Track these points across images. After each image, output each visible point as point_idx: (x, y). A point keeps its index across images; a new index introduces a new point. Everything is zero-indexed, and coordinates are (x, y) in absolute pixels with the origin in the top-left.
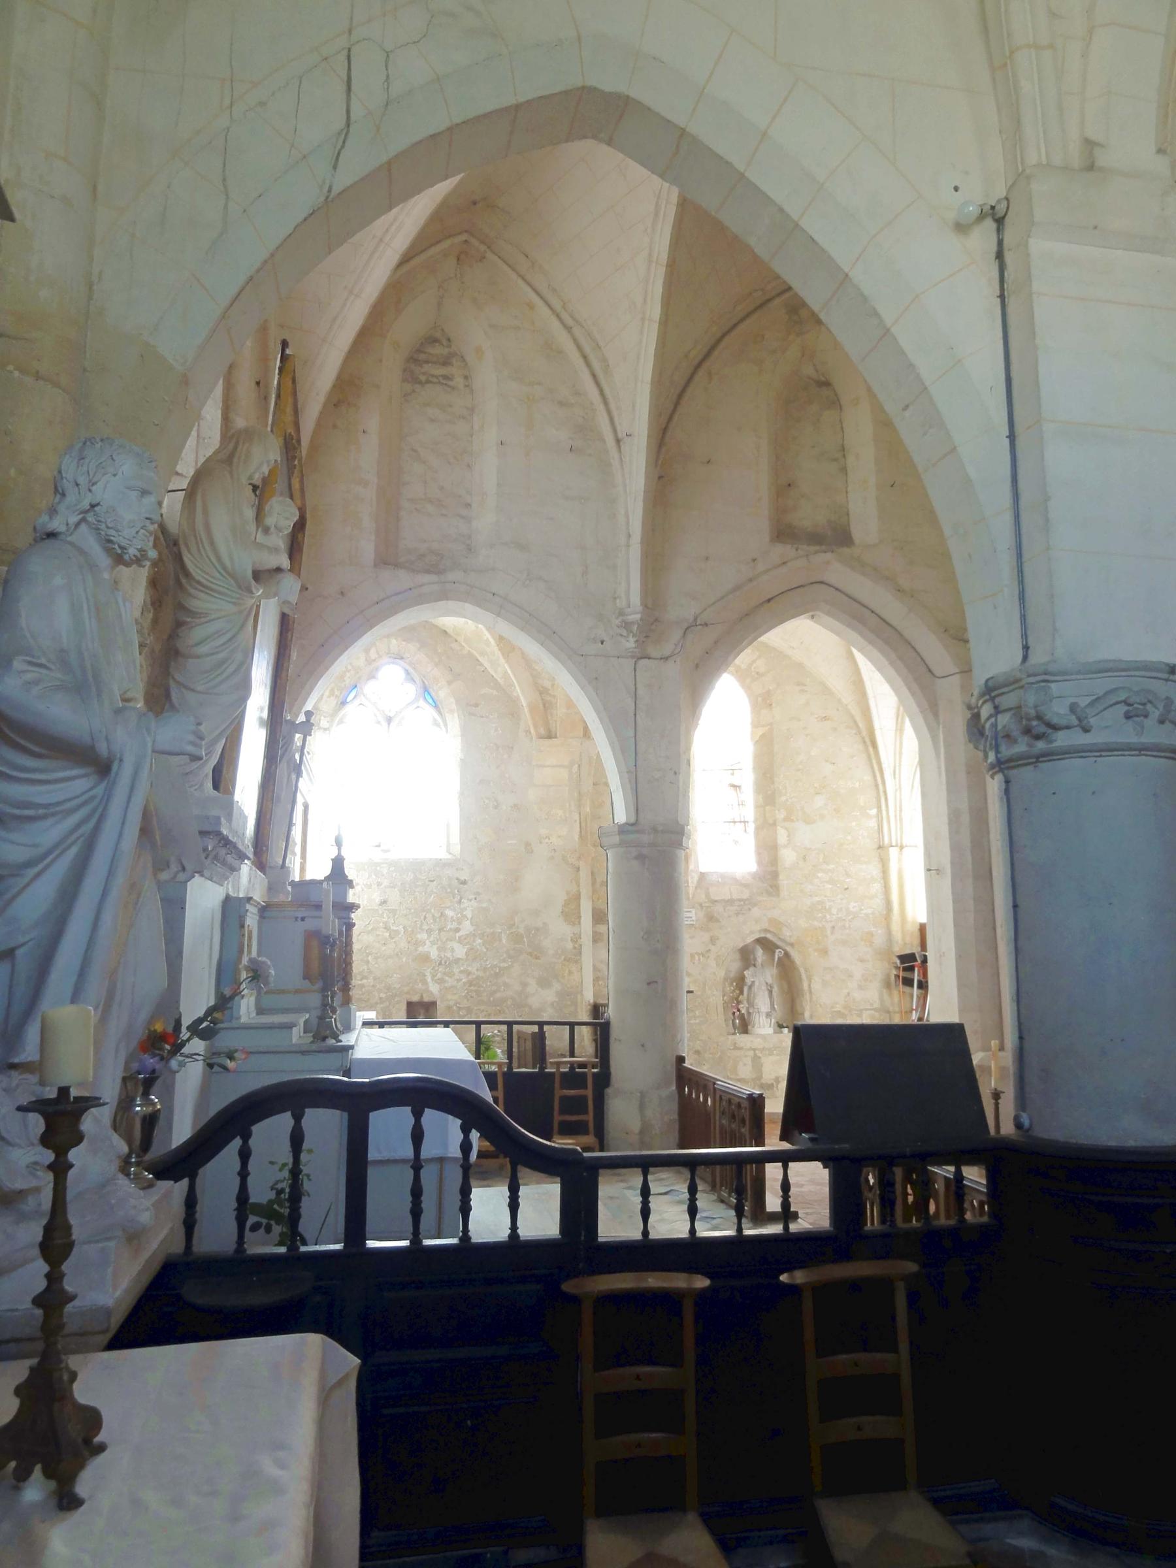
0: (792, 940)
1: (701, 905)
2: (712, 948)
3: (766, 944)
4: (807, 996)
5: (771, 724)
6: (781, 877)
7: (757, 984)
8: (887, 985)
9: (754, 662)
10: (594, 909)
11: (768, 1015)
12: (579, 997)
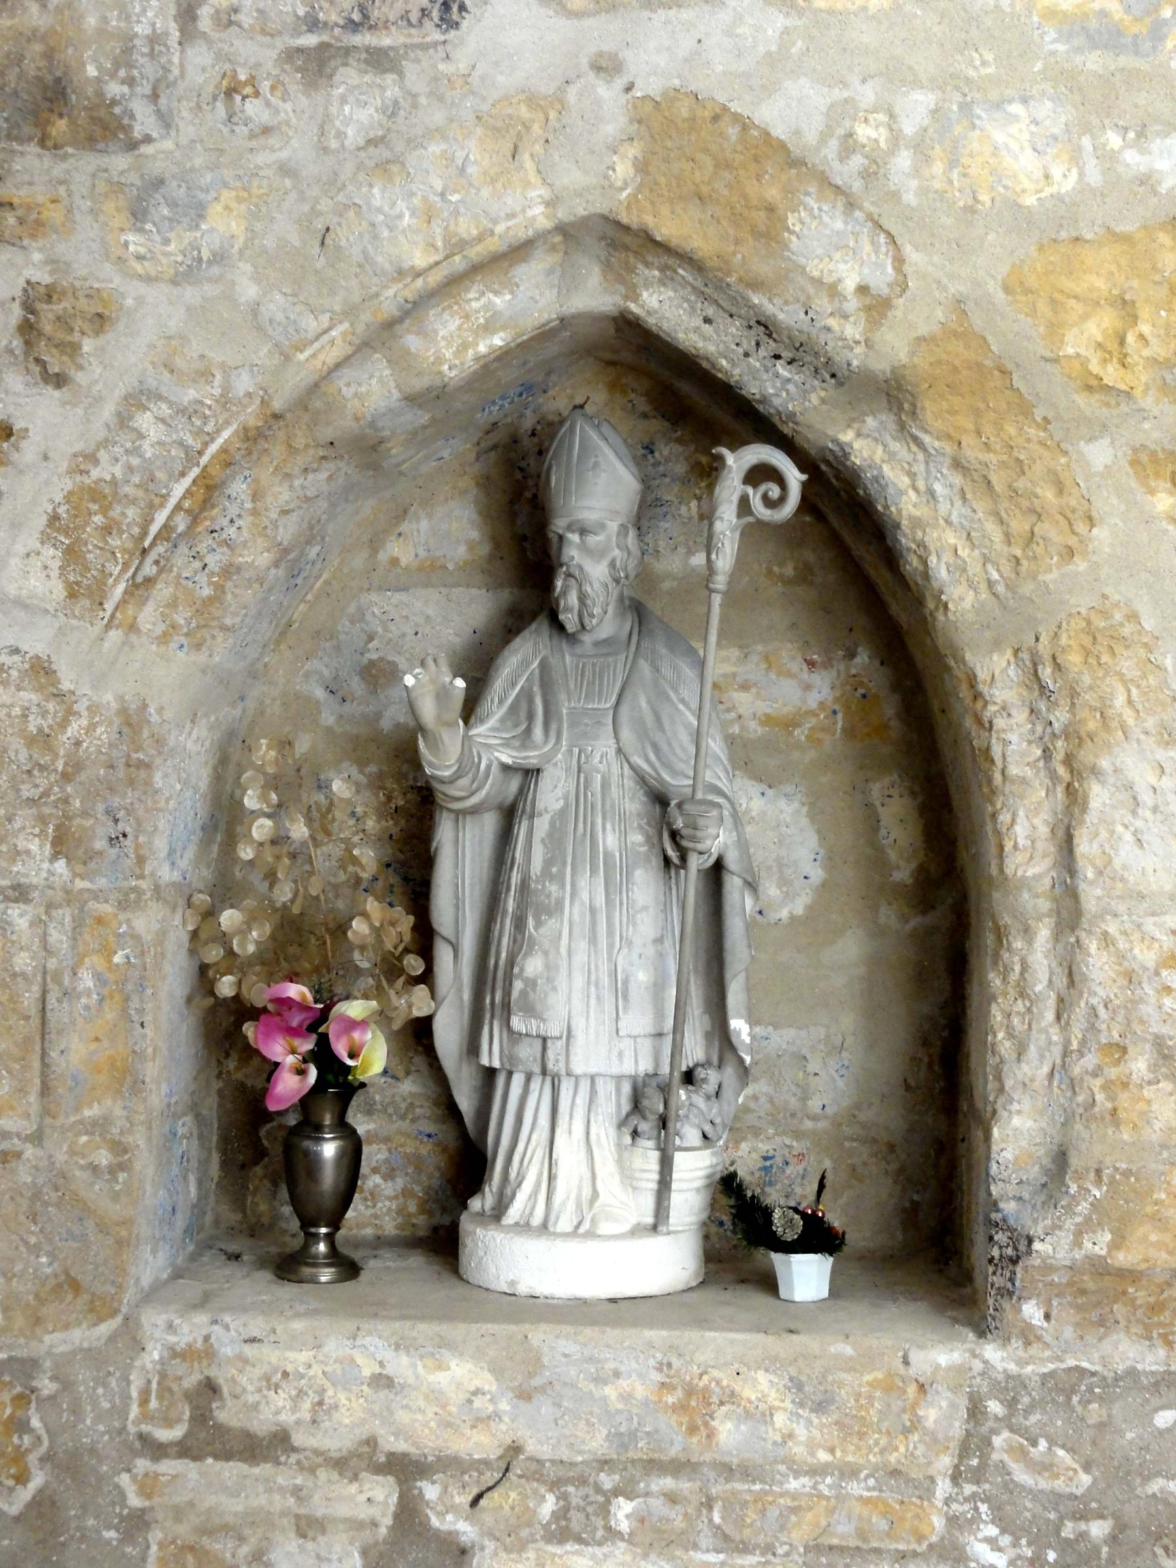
0: (894, 347)
3: (688, 407)
7: (551, 795)
11: (649, 1111)
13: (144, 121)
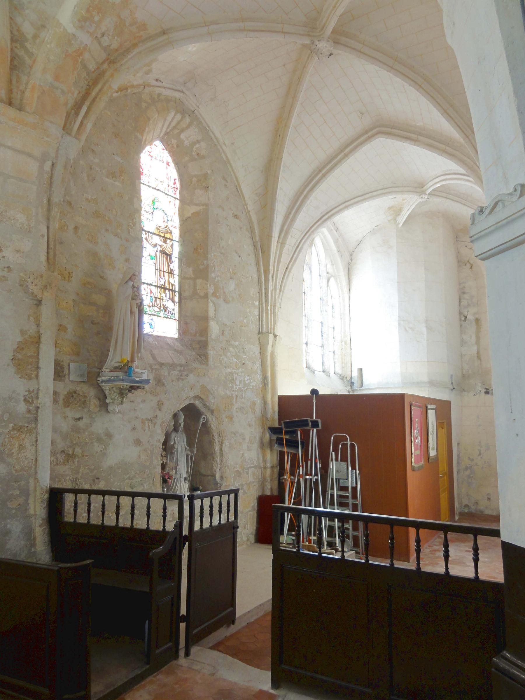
1: (151, 367)
2: (158, 413)
4: (218, 459)
5: (207, 205)
6: (210, 347)
8: (262, 445)
9: (198, 142)
10: (55, 360)
12: (32, 481)
13: (166, 384)
